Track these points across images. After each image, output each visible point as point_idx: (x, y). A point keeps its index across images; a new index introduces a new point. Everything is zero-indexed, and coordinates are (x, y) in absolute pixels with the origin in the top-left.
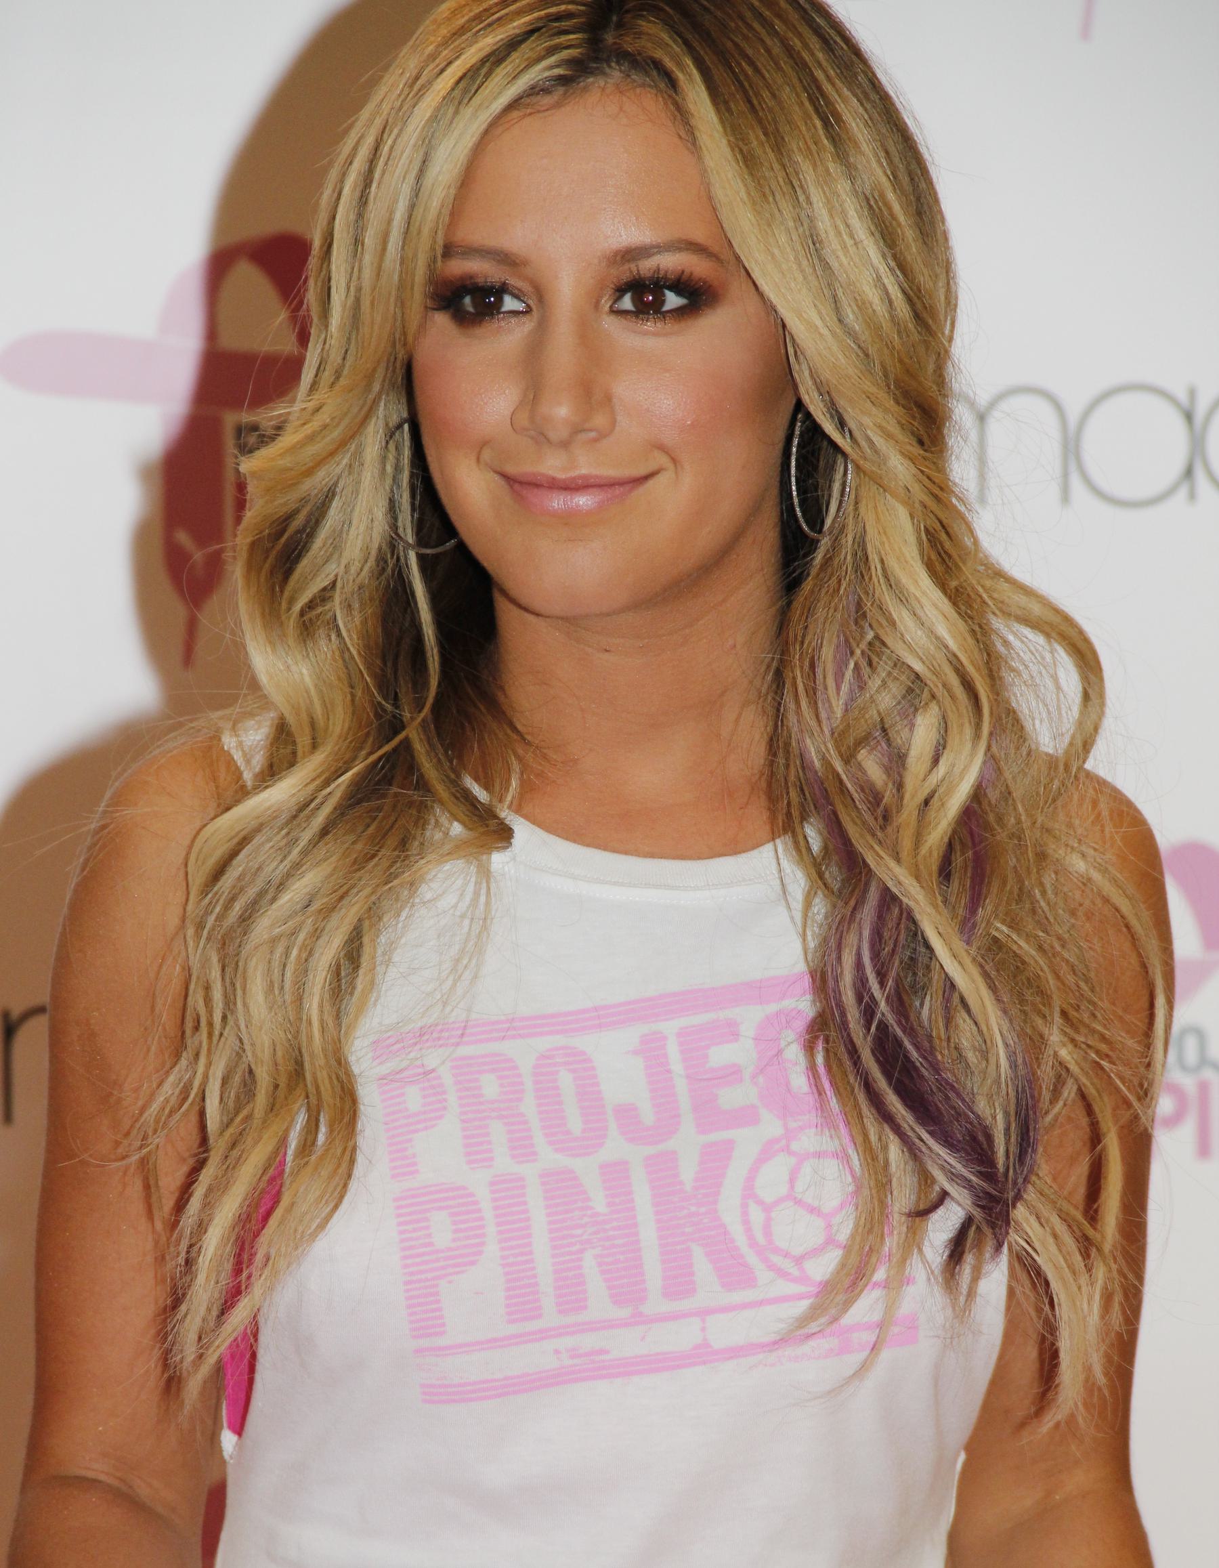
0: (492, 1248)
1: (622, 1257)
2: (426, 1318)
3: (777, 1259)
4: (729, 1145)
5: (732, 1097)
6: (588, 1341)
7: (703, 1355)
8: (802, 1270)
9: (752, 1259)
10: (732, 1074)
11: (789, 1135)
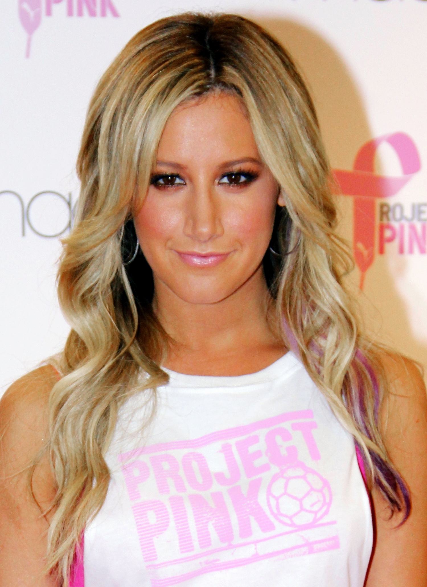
0: (172, 524)
1: (223, 524)
2: (150, 553)
3: (282, 518)
4: (260, 480)
5: (258, 463)
6: (211, 558)
7: (256, 558)
8: (292, 521)
9: (272, 519)
10: (258, 454)
11: (283, 472)
